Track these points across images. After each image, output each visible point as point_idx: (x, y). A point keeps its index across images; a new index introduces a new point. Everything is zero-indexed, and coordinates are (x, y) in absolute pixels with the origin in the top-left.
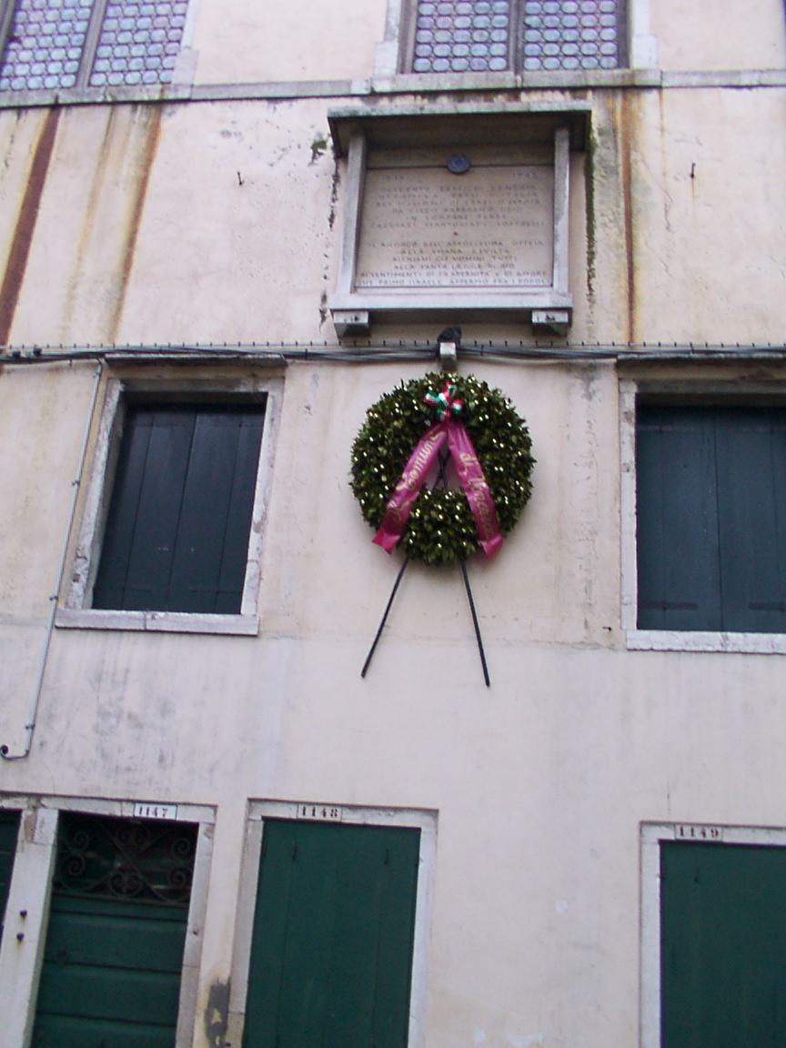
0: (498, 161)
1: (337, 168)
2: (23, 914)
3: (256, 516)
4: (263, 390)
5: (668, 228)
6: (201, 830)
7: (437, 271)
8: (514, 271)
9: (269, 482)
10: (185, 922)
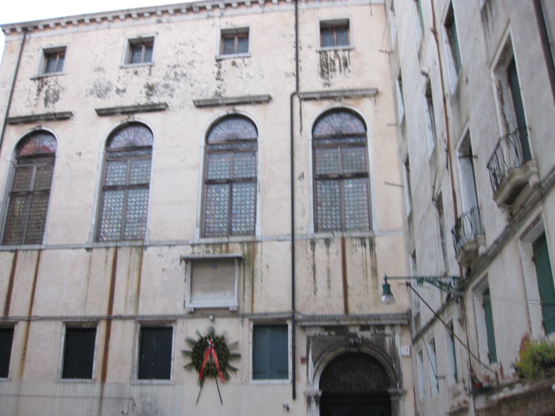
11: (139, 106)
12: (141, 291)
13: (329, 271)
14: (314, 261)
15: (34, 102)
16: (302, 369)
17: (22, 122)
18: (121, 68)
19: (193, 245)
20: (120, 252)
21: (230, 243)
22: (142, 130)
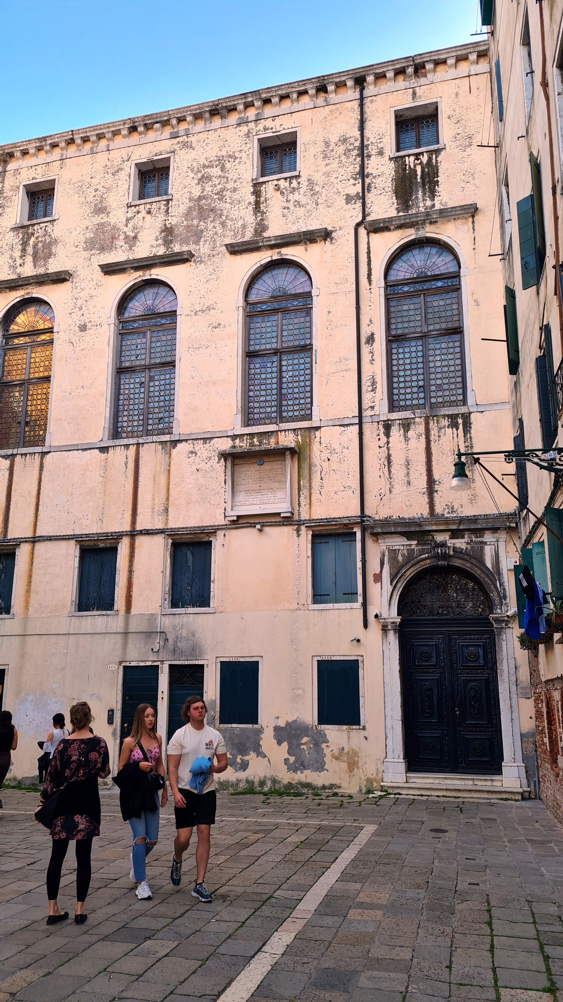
0: (271, 460)
1: (226, 464)
2: (163, 692)
3: (212, 579)
4: (211, 539)
5: (321, 479)
6: (205, 666)
7: (255, 499)
8: (277, 498)
9: (215, 568)
10: (203, 690)
11: (155, 257)
12: (171, 499)
13: (408, 463)
14: (388, 449)
15: (19, 261)
16: (374, 589)
17: (6, 288)
18: (129, 206)
19: (234, 437)
20: (143, 451)
21: (281, 431)
22: (163, 291)
